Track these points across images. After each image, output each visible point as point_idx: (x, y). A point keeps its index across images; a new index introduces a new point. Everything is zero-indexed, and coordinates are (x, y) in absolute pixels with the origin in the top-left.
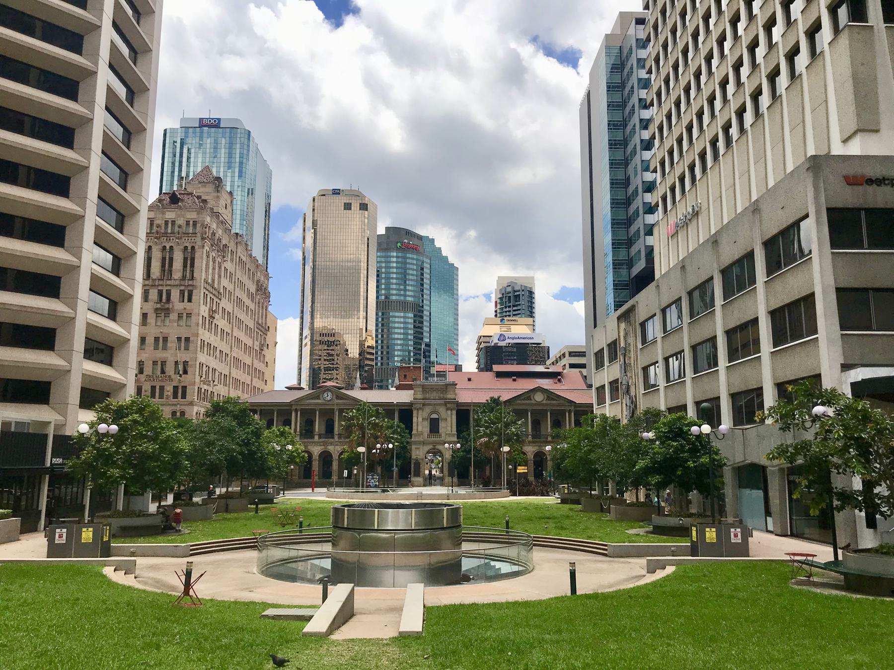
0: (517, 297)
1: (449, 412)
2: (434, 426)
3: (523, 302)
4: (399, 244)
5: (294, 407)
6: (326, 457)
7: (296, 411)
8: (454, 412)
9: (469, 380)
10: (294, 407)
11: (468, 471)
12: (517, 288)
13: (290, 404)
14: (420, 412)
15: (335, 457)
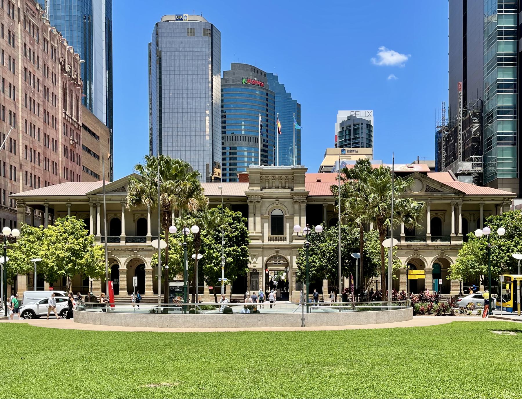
0: (356, 131)
1: (296, 206)
2: (277, 226)
3: (362, 133)
4: (244, 80)
5: (91, 202)
6: (139, 270)
7: (95, 207)
8: (303, 206)
9: (319, 181)
10: (91, 202)
11: (322, 284)
12: (356, 123)
13: (87, 198)
14: (258, 205)
15: (148, 267)
